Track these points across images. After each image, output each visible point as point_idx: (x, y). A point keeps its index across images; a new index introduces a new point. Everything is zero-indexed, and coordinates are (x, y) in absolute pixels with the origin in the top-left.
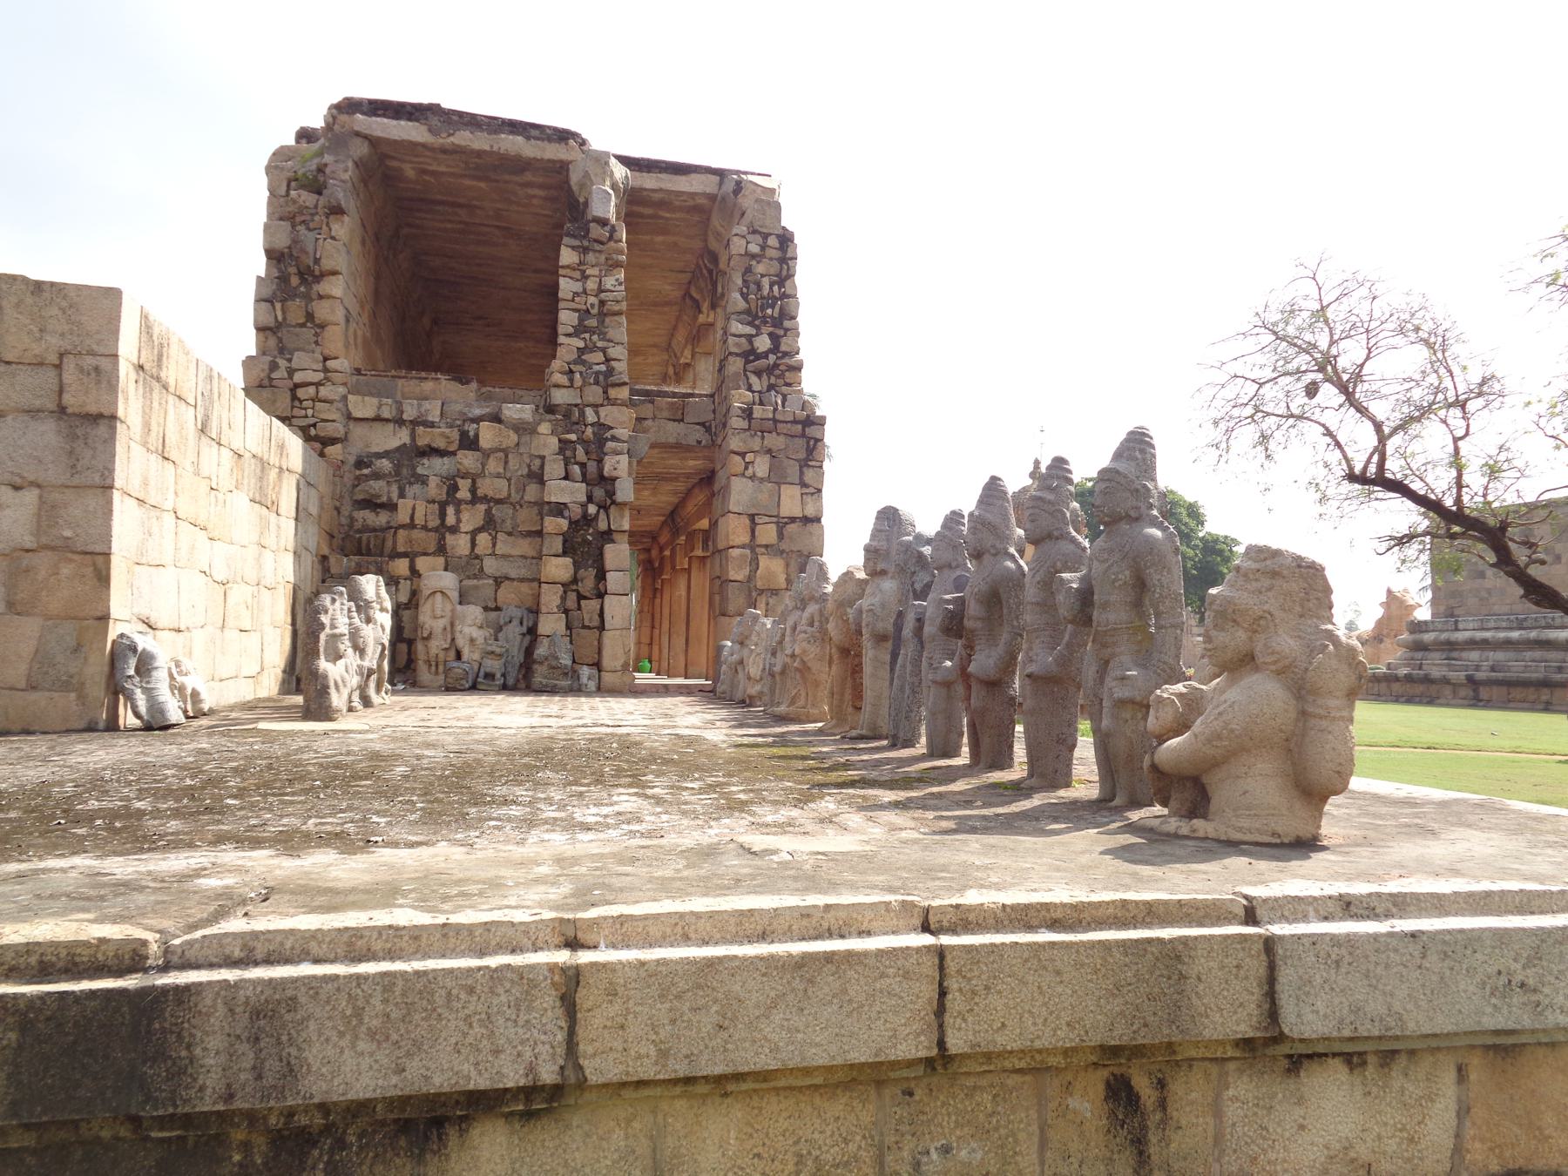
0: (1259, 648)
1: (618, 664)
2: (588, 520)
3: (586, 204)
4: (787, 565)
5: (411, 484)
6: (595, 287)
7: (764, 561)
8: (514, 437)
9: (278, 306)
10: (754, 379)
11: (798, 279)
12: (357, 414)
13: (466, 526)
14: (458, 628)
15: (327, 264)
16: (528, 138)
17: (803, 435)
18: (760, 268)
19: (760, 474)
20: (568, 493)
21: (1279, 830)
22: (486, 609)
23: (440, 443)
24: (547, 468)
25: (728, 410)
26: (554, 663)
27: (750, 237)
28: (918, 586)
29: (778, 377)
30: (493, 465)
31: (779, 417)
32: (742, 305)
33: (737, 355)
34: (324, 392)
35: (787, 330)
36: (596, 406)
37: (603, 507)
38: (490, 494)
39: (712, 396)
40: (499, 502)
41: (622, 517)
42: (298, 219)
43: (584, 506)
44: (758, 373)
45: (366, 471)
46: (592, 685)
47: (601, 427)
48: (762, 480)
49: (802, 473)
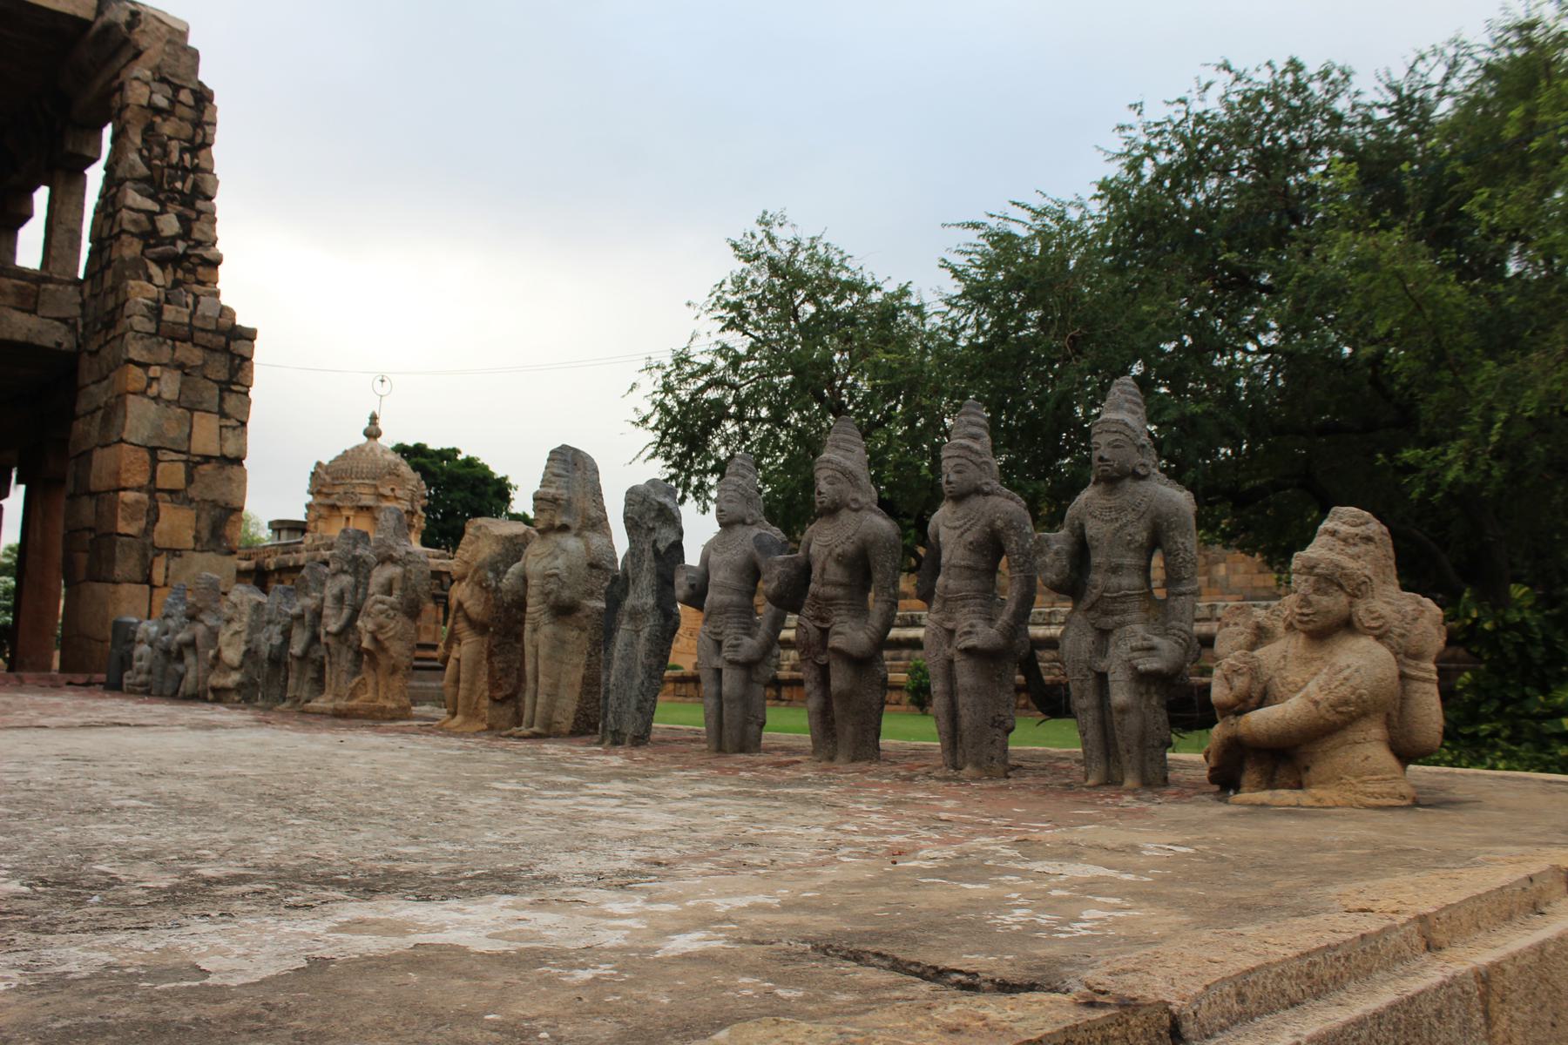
0: (1361, 609)
4: (198, 518)
10: (154, 270)
17: (226, 349)
18: (167, 128)
19: (166, 396)
27: (155, 86)
28: (662, 546)
31: (197, 323)
32: (142, 170)
33: (133, 235)
35: (200, 212)
44: (161, 262)
48: (169, 402)
49: (222, 399)
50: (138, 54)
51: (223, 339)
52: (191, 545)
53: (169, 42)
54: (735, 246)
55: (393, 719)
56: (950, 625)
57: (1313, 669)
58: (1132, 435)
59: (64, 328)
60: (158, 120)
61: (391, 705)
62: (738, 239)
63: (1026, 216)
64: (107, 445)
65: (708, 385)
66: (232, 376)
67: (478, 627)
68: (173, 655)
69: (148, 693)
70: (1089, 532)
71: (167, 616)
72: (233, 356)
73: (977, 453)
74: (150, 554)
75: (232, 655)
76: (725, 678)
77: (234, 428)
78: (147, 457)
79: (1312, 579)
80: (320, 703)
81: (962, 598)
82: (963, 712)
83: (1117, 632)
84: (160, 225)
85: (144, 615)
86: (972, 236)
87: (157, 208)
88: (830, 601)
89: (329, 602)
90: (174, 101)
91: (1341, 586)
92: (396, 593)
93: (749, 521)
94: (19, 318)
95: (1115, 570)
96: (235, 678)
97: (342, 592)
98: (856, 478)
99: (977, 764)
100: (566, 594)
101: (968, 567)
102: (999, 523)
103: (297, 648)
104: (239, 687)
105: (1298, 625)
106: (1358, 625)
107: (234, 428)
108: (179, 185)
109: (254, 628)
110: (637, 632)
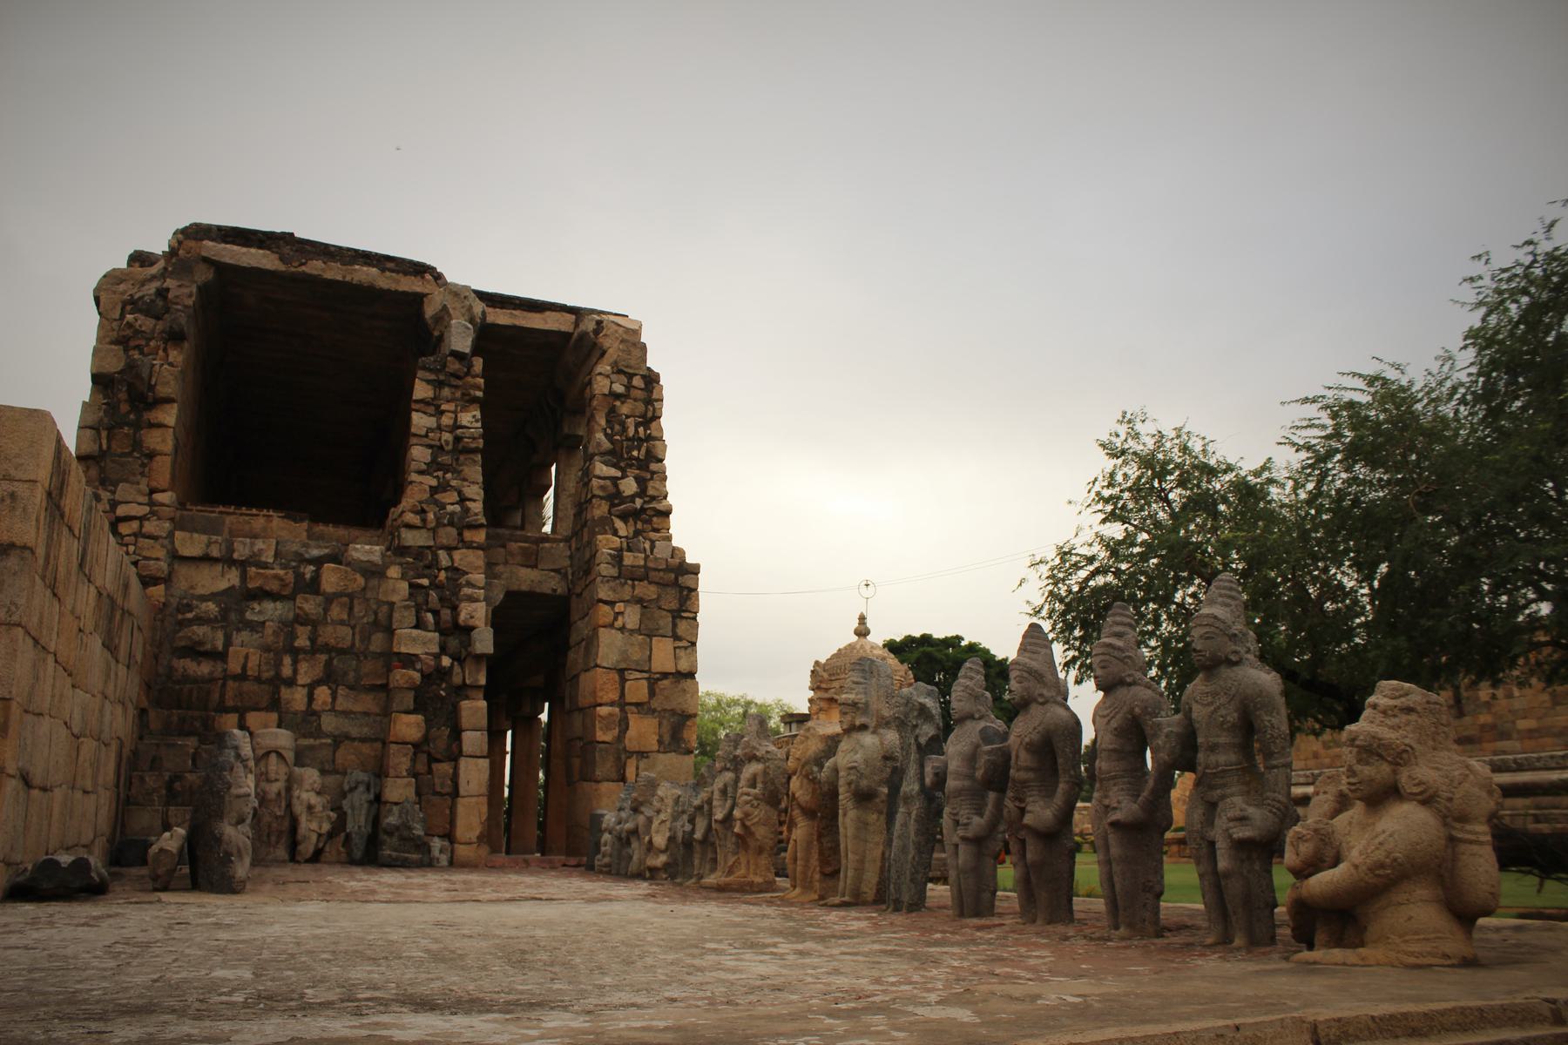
0: (1403, 779)
1: (474, 835)
2: (444, 674)
3: (441, 338)
5: (239, 630)
6: (451, 422)
7: (633, 720)
8: (361, 581)
9: (104, 434)
10: (619, 524)
11: (664, 421)
12: (186, 552)
13: (303, 679)
14: (296, 793)
15: (163, 391)
16: (383, 270)
17: (676, 584)
18: (625, 409)
20: (418, 642)
21: (1447, 951)
22: (323, 772)
23: (274, 586)
24: (396, 615)
25: (594, 556)
26: (406, 833)
27: (614, 377)
28: (923, 740)
30: (336, 612)
31: (651, 565)
32: (607, 445)
33: (602, 498)
34: (149, 527)
35: (653, 473)
36: (449, 549)
37: (456, 658)
38: (332, 642)
39: (567, 540)
40: (342, 652)
41: (478, 671)
42: (132, 344)
43: (437, 657)
44: (624, 517)
45: (190, 616)
46: (444, 860)
47: (453, 569)
48: (632, 630)
49: (675, 625)
50: (603, 353)
52: (656, 747)
53: (622, 341)
54: (1103, 446)
55: (760, 892)
56: (1106, 802)
59: (558, 577)
60: (618, 403)
61: (758, 880)
62: (1105, 438)
63: (1361, 384)
65: (1093, 574)
67: (809, 813)
68: (624, 840)
69: (609, 873)
70: (1194, 715)
71: (620, 809)
72: (682, 588)
73: (1119, 649)
76: (961, 852)
78: (617, 677)
80: (711, 880)
81: (1114, 778)
83: (1221, 805)
84: (622, 488)
85: (610, 808)
86: (1311, 410)
87: (619, 474)
88: (1024, 784)
89: (716, 795)
90: (629, 387)
92: (759, 785)
95: (1213, 748)
96: (663, 858)
97: (725, 786)
98: (1041, 676)
99: (1130, 926)
100: (864, 783)
101: (1114, 750)
102: (1137, 710)
103: (698, 835)
104: (666, 866)
108: (635, 453)
109: (675, 818)
110: (909, 814)
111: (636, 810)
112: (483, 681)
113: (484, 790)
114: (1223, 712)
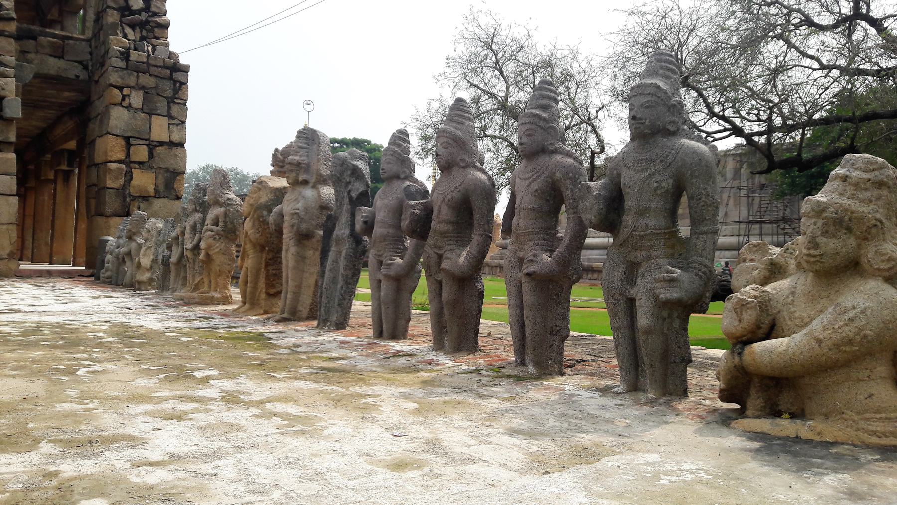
0: (869, 253)
7: (136, 173)
10: (128, 30)
17: (171, 78)
25: (107, 52)
28: (354, 195)
29: (148, 31)
31: (151, 62)
33: (114, 9)
39: (88, 41)
44: (132, 27)
49: (169, 108)
51: (169, 72)
56: (521, 254)
57: (819, 307)
58: (663, 96)
64: (101, 136)
66: (175, 94)
68: (120, 261)
69: (110, 283)
70: (623, 180)
71: (119, 237)
72: (175, 82)
73: (545, 119)
74: (128, 200)
75: (146, 262)
77: (177, 125)
78: (123, 142)
79: (820, 223)
82: (527, 322)
89: (188, 230)
91: (849, 230)
93: (402, 176)
94: (52, 60)
96: (146, 276)
97: (195, 224)
100: (304, 226)
101: (533, 210)
105: (805, 265)
106: (865, 266)
107: (177, 125)
109: (158, 245)
110: (340, 253)
111: (130, 238)
112: (13, 138)
113: (14, 219)
114: (658, 178)
